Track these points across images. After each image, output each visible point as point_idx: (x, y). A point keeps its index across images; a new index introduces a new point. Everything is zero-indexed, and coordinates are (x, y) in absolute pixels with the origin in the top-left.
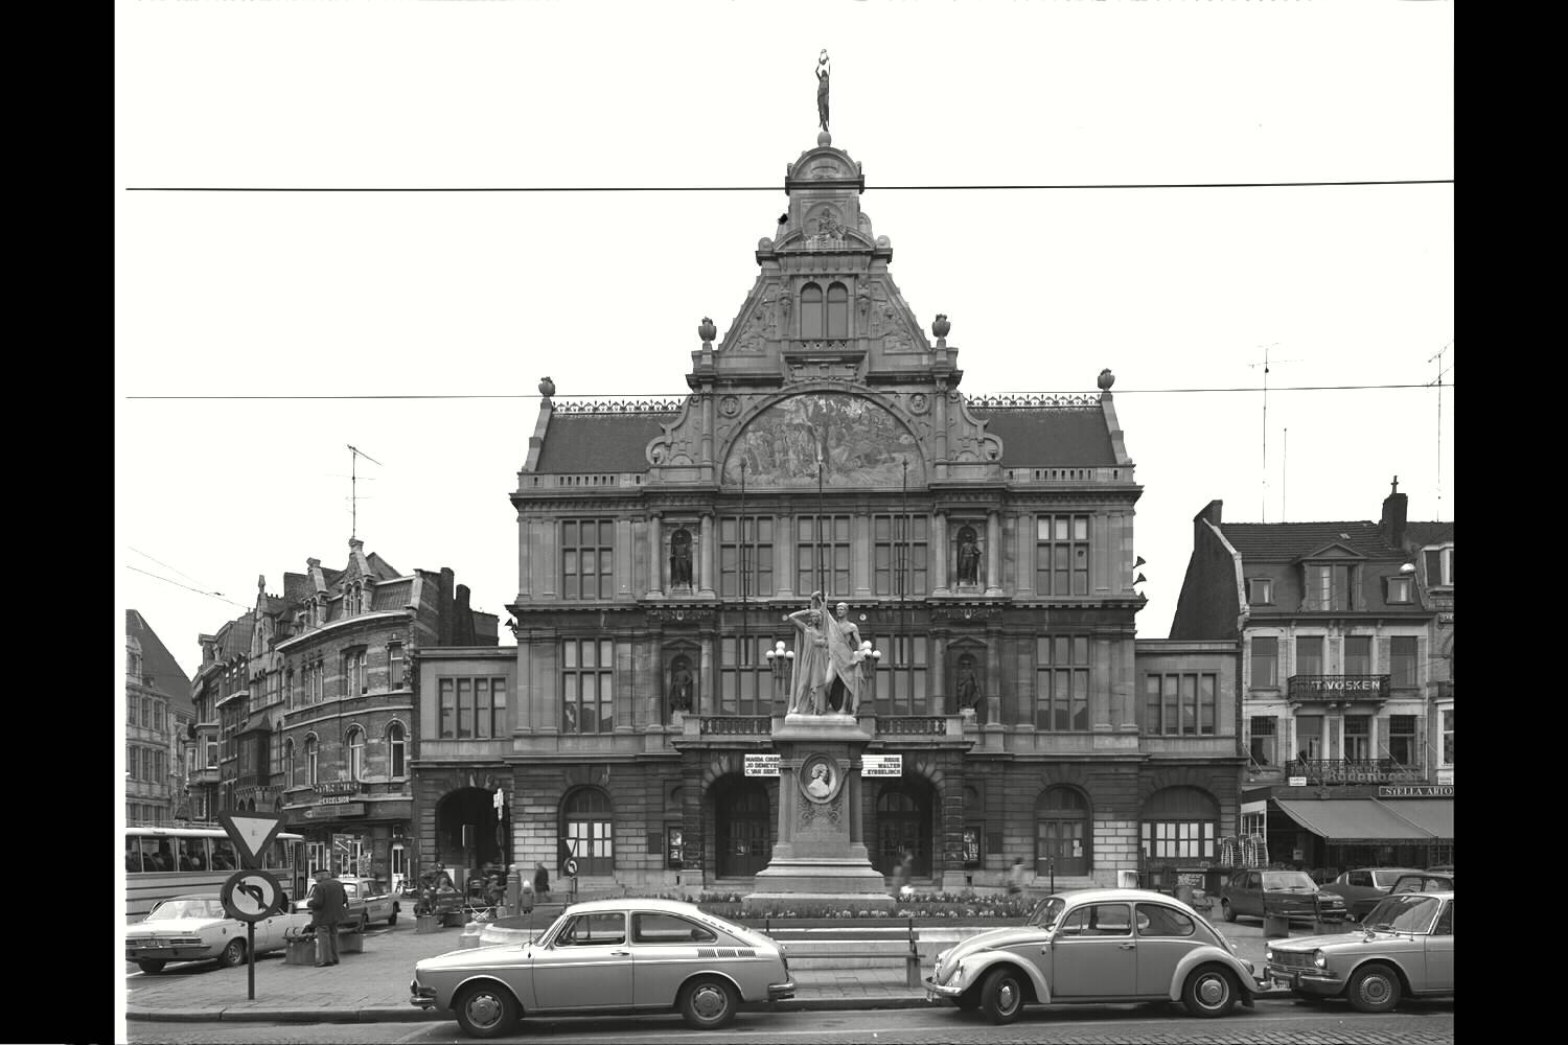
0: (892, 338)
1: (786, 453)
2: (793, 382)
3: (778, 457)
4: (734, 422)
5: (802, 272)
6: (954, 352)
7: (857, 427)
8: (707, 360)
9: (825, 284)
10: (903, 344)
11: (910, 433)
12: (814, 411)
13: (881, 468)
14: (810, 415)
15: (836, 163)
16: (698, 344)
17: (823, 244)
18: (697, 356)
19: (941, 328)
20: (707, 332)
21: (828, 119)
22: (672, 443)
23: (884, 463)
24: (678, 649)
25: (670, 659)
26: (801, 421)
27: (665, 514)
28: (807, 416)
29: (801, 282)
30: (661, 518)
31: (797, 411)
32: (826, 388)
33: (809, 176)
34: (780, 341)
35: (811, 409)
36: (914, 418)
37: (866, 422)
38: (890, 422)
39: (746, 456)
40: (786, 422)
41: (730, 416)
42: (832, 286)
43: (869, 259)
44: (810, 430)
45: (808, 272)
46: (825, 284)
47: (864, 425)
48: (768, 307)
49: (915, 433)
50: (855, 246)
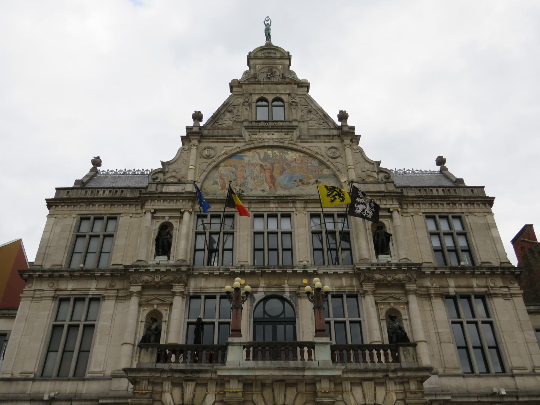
1: (246, 178)
2: (251, 140)
4: (209, 161)
5: (256, 92)
6: (353, 128)
7: (293, 164)
9: (270, 98)
10: (320, 124)
11: (328, 167)
12: (264, 156)
13: (310, 186)
16: (191, 123)
17: (269, 77)
19: (343, 116)
20: (198, 117)
21: (270, 37)
22: (167, 172)
24: (153, 305)
25: (146, 313)
26: (256, 162)
27: (156, 211)
28: (260, 159)
29: (256, 97)
30: (152, 213)
31: (254, 156)
32: (271, 144)
34: (243, 122)
35: (262, 156)
36: (331, 160)
37: (299, 162)
38: (315, 163)
39: (218, 180)
40: (246, 162)
41: (208, 157)
42: (274, 100)
43: (296, 86)
44: (261, 166)
45: (260, 92)
46: (270, 98)
49: (332, 166)
50: (288, 80)
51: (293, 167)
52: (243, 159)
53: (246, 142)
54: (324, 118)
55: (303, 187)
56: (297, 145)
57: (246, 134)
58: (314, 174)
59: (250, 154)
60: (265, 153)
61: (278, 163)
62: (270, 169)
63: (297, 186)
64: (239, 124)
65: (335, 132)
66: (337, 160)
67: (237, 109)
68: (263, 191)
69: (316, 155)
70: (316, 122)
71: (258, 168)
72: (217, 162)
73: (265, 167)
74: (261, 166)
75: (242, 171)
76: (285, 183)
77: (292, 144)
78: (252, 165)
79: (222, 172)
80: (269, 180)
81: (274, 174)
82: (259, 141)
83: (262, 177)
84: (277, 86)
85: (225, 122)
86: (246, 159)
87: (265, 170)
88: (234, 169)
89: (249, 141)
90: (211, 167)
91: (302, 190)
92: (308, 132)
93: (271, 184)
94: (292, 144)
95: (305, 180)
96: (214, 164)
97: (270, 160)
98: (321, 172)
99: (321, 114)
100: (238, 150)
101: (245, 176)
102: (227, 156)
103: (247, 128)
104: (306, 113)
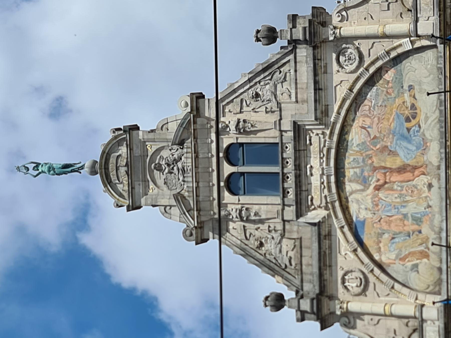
0: (278, 93)
3: (410, 226)
7: (374, 132)
8: (306, 305)
9: (228, 169)
12: (357, 182)
13: (418, 105)
14: (359, 187)
15: (112, 160)
18: (302, 317)
23: (414, 97)
26: (369, 197)
28: (363, 190)
31: (358, 201)
33: (123, 187)
37: (368, 122)
39: (409, 264)
44: (378, 188)
46: (228, 169)
47: (372, 123)
48: (251, 234)
49: (379, 63)
51: (380, 132)
52: (364, 221)
53: (329, 215)
54: (270, 71)
55: (421, 117)
56: (335, 123)
57: (316, 215)
58: (393, 95)
59: (353, 208)
60: (350, 181)
61: (371, 158)
62: (385, 174)
63: (420, 127)
64: (287, 227)
65: (303, 52)
66: (365, 53)
67: (252, 231)
68: (430, 186)
69: (355, 90)
70: (279, 86)
71: (381, 194)
72: (372, 266)
73: (381, 182)
74: (378, 188)
75: (389, 223)
76: (414, 148)
77: (332, 133)
78: (377, 205)
79: (393, 256)
80: (408, 175)
81: (394, 167)
82: (326, 191)
83: (402, 187)
84: (201, 156)
85: (284, 253)
86: (363, 215)
87: (386, 183)
88: (386, 236)
89: (326, 208)
90: (383, 277)
91: (427, 118)
92: (303, 101)
93: (417, 172)
94: (332, 133)
95: (406, 112)
96: (377, 271)
97: (366, 174)
98: (388, 82)
99: (262, 76)
100: (346, 229)
101: (400, 216)
102: (359, 250)
103: (299, 214)
104: (260, 103)
